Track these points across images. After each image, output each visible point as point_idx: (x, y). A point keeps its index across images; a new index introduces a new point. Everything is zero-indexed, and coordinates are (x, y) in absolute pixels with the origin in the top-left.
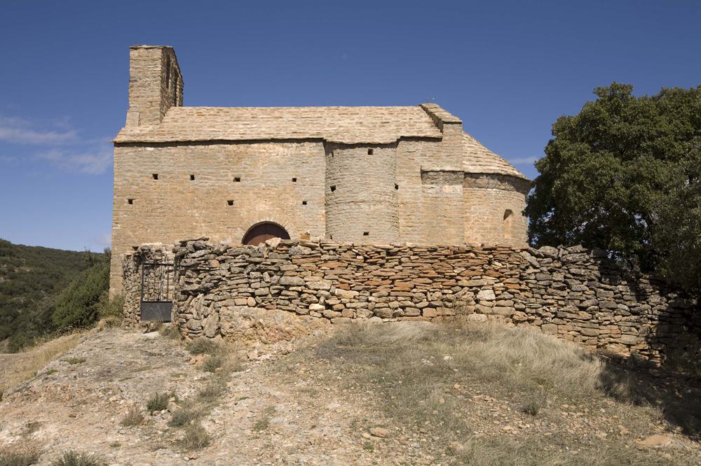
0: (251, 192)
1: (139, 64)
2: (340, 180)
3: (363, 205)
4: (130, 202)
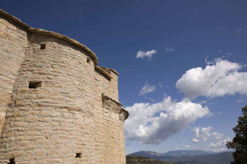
2: (51, 77)
3: (78, 115)
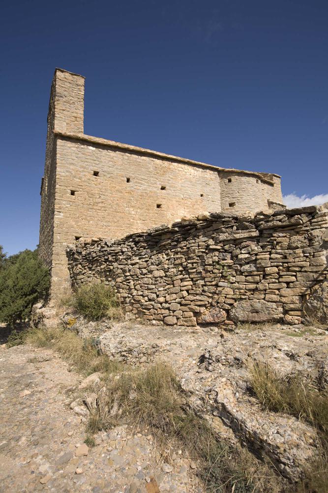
0: (174, 199)
1: (64, 85)
2: (239, 198)
4: (73, 193)
